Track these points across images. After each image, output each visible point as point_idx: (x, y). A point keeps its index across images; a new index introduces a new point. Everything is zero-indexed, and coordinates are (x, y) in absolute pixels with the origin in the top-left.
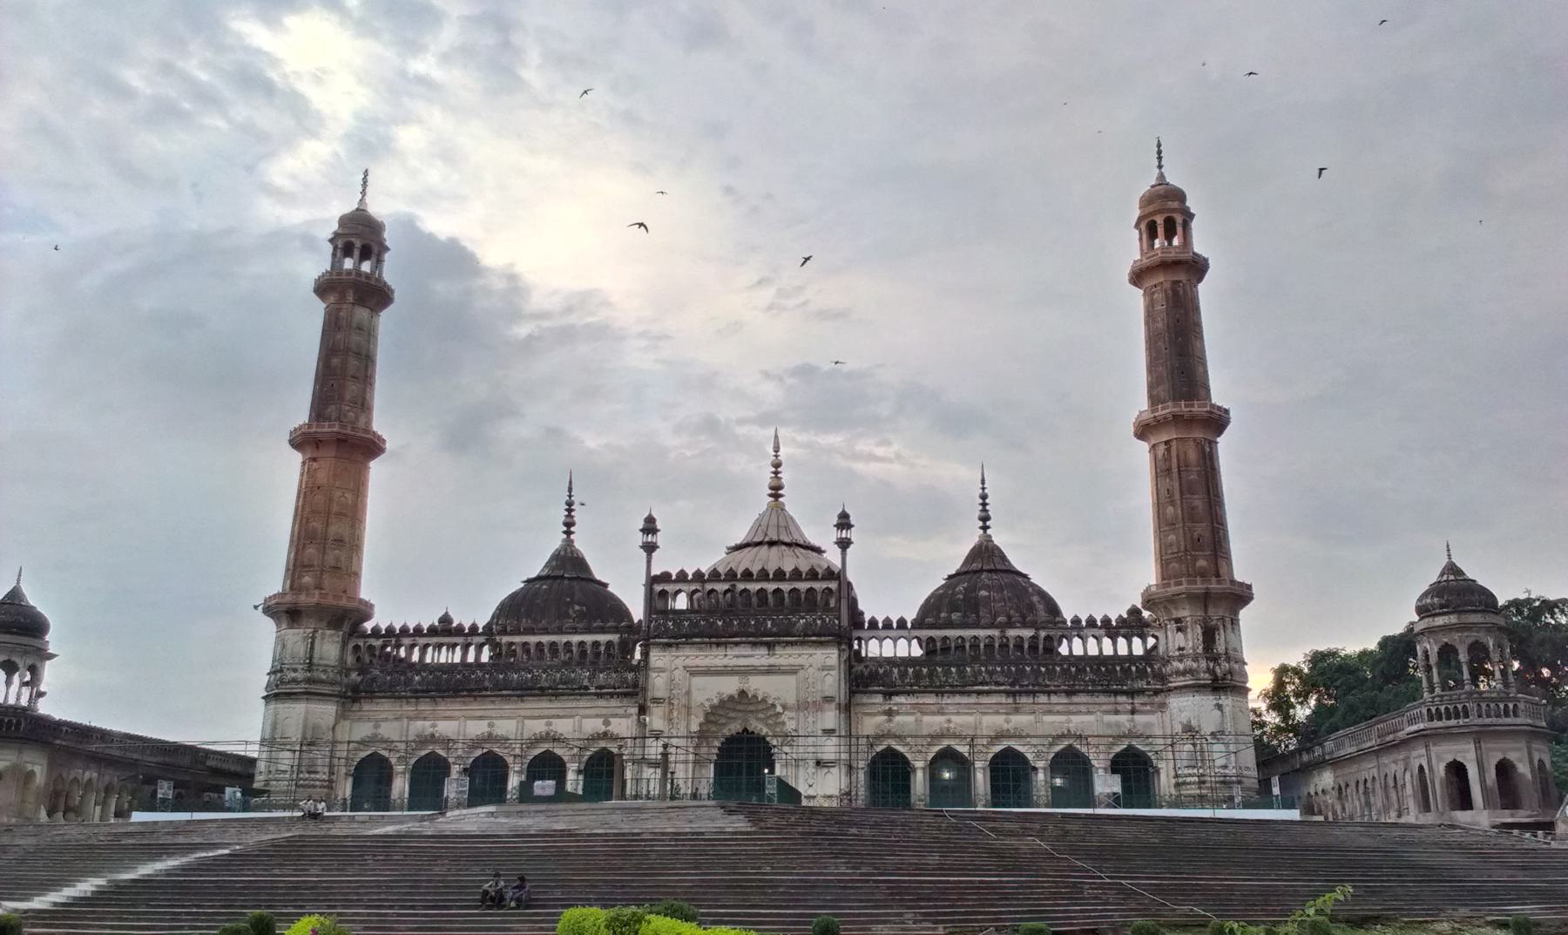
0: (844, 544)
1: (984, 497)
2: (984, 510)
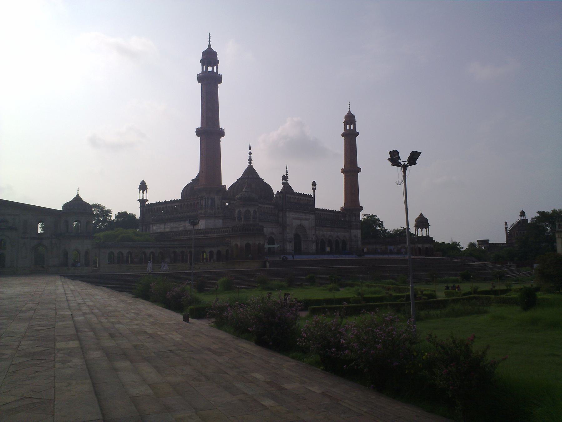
0: (314, 189)
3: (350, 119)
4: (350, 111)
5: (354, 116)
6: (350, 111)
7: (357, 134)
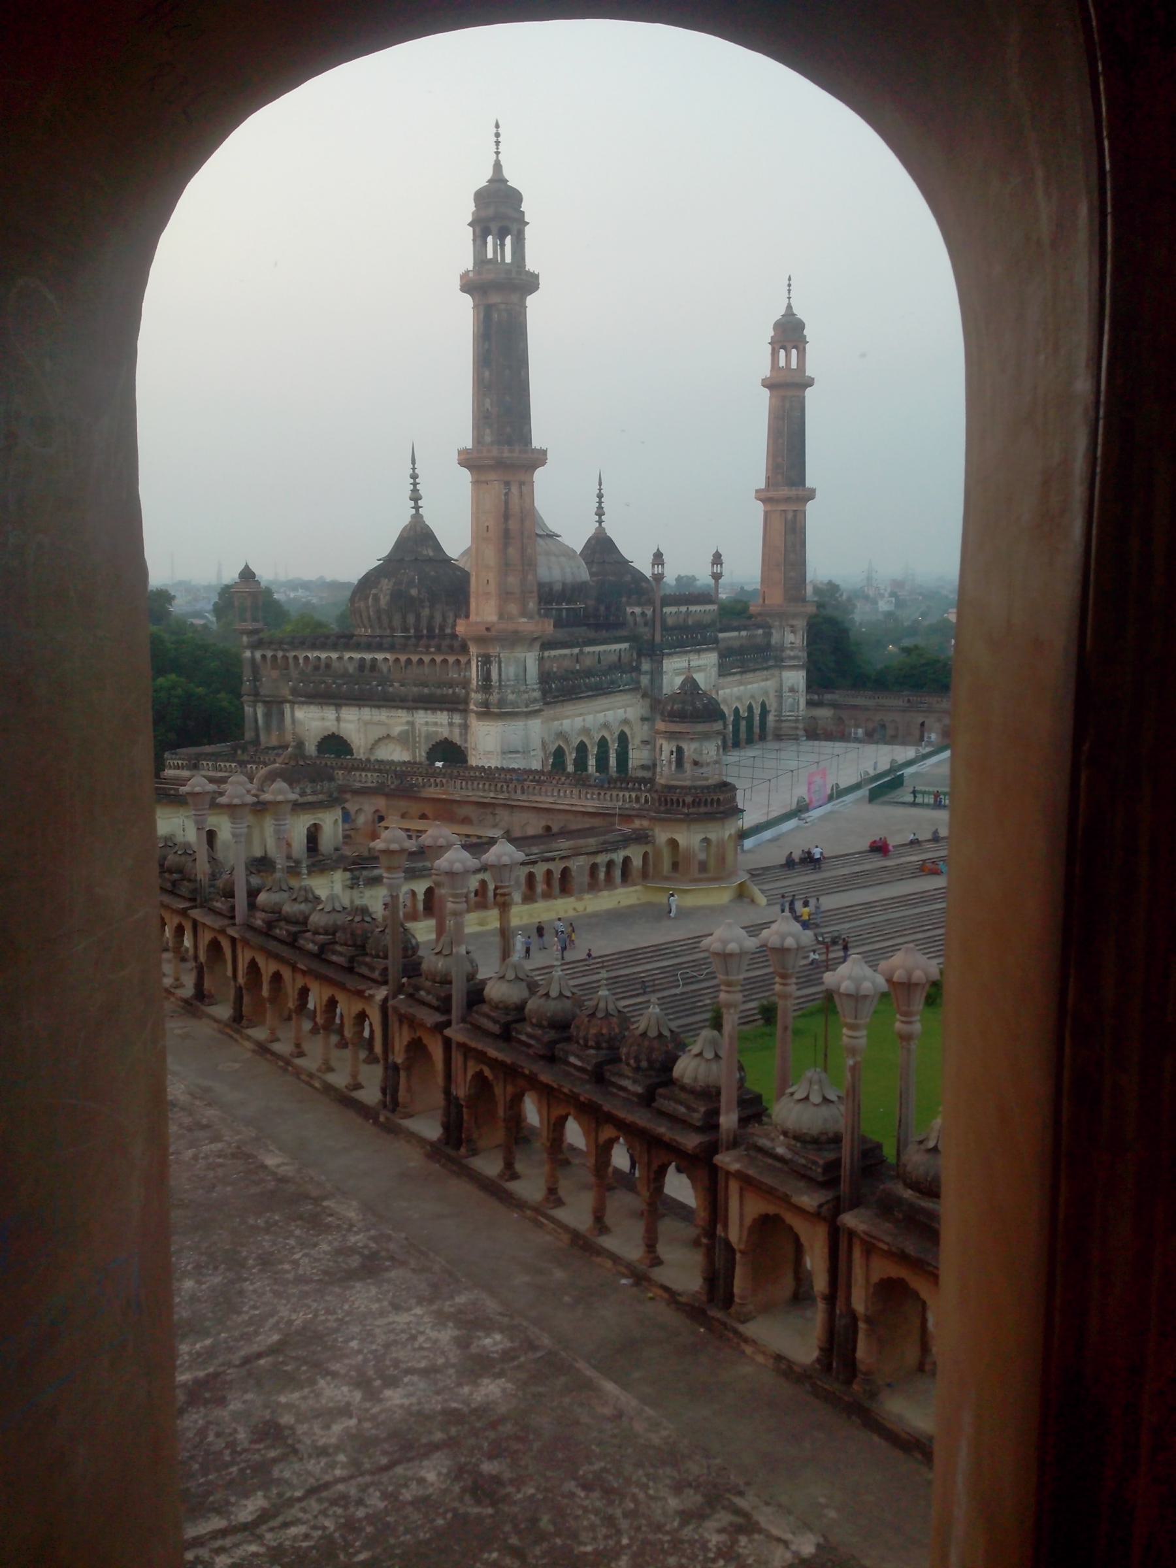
0: (717, 577)
2: (600, 508)
3: (789, 333)
4: (789, 307)
5: (800, 326)
6: (789, 307)
7: (810, 383)
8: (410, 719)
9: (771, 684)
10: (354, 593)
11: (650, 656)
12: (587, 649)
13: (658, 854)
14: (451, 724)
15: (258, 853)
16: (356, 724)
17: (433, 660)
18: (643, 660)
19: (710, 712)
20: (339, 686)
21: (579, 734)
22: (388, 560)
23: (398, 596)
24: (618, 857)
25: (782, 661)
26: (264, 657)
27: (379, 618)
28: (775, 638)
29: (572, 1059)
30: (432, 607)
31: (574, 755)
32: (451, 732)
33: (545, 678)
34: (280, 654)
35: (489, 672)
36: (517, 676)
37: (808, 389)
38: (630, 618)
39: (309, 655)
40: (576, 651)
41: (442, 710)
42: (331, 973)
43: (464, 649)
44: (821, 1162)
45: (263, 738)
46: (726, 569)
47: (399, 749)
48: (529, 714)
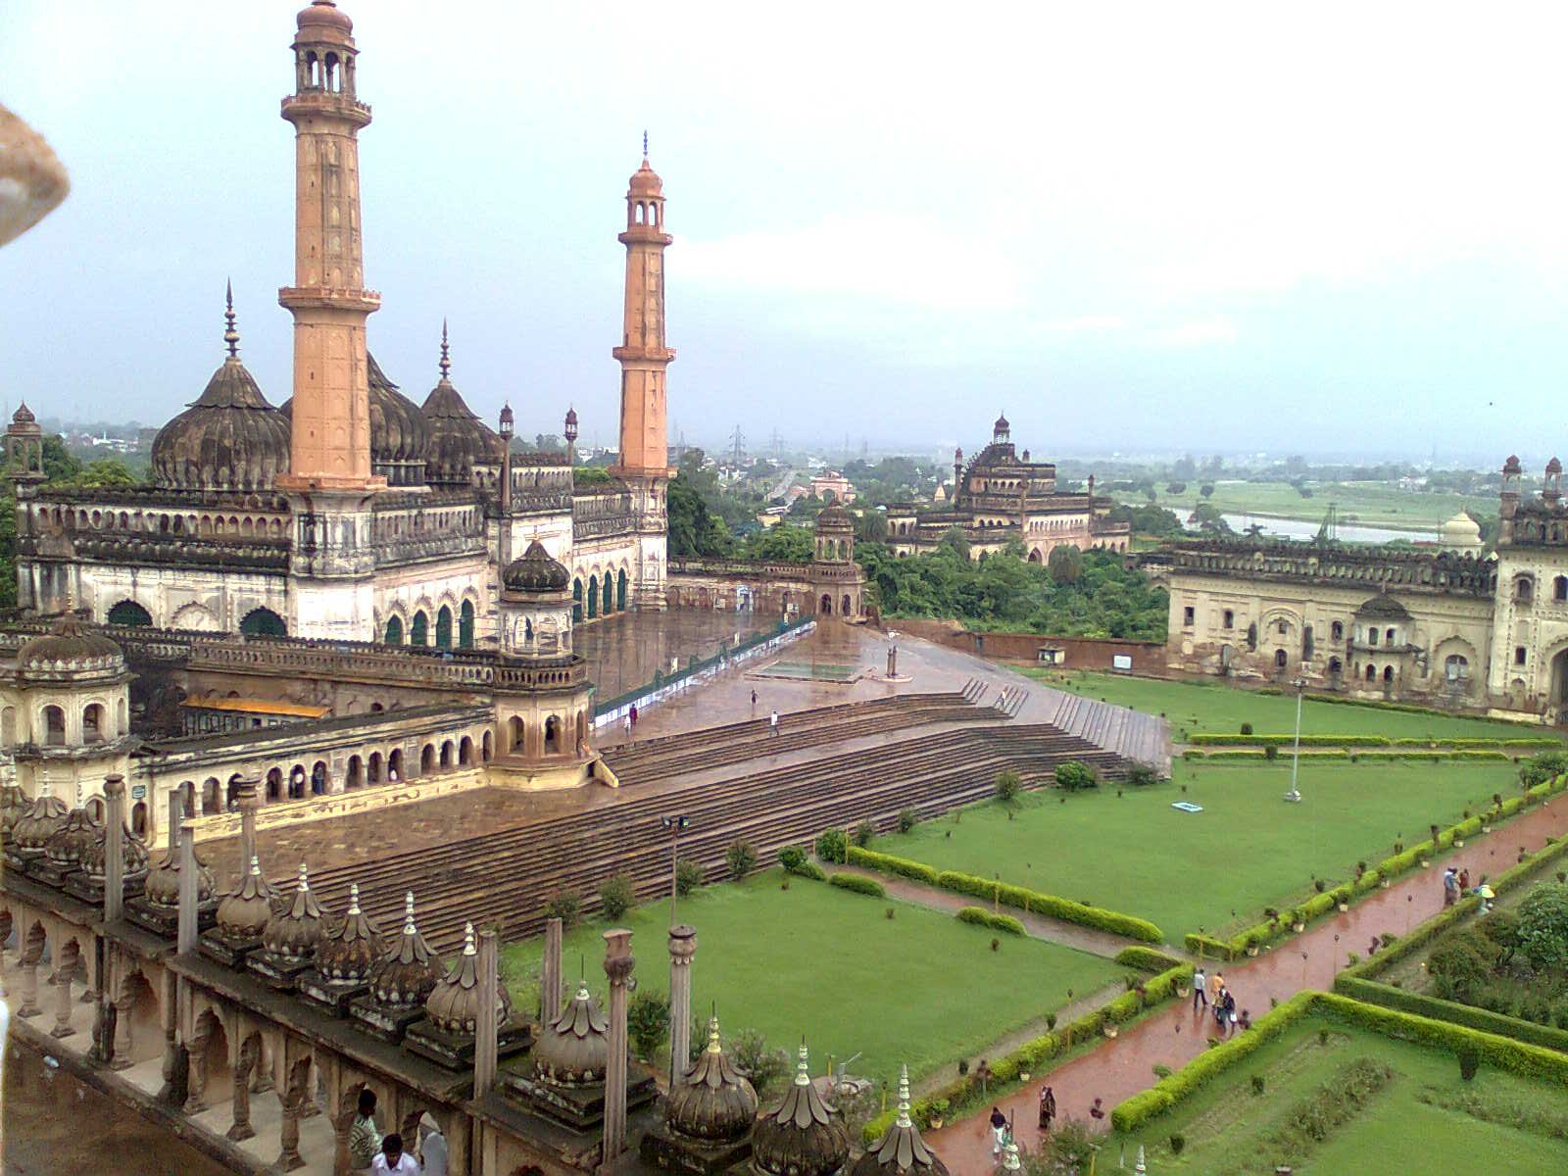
0: (571, 437)
1: (445, 347)
2: (445, 358)
4: (645, 163)
5: (656, 183)
6: (645, 163)
8: (222, 585)
9: (630, 553)
10: (156, 445)
11: (498, 519)
12: (427, 511)
13: (500, 736)
14: (269, 591)
15: (22, 740)
16: (155, 591)
17: (248, 520)
18: (490, 523)
19: (557, 581)
20: (136, 547)
21: (417, 603)
22: (199, 407)
23: (206, 445)
24: (455, 738)
25: (642, 527)
26: (43, 511)
27: (187, 471)
28: (635, 503)
29: (314, 992)
30: (248, 461)
31: (411, 626)
32: (269, 599)
33: (376, 543)
34: (64, 508)
35: (312, 534)
36: (345, 538)
37: (667, 248)
38: (476, 481)
39: (100, 510)
40: (414, 512)
41: (258, 574)
42: (34, 894)
43: (284, 507)
44: (585, 1103)
45: (40, 605)
46: (580, 429)
47: (207, 618)
48: (357, 581)
